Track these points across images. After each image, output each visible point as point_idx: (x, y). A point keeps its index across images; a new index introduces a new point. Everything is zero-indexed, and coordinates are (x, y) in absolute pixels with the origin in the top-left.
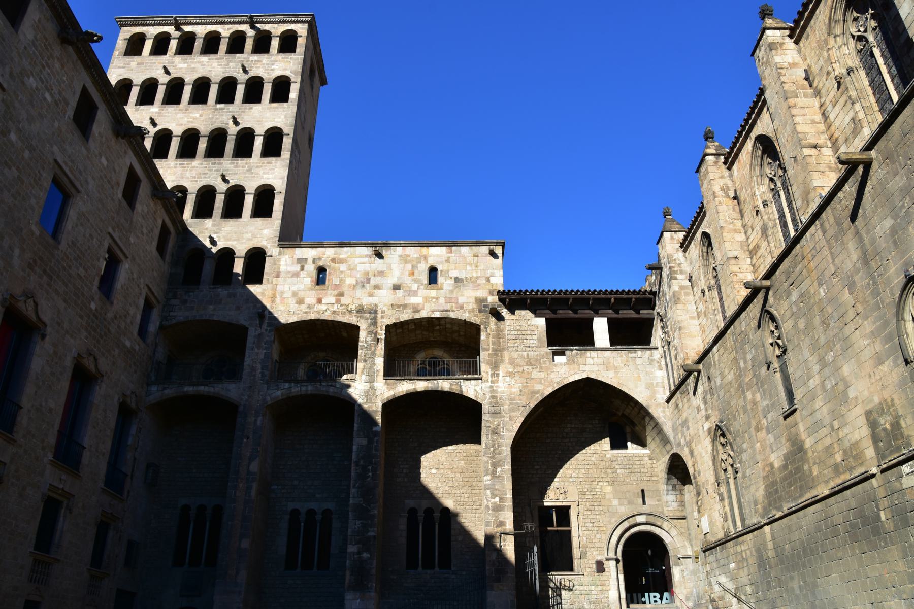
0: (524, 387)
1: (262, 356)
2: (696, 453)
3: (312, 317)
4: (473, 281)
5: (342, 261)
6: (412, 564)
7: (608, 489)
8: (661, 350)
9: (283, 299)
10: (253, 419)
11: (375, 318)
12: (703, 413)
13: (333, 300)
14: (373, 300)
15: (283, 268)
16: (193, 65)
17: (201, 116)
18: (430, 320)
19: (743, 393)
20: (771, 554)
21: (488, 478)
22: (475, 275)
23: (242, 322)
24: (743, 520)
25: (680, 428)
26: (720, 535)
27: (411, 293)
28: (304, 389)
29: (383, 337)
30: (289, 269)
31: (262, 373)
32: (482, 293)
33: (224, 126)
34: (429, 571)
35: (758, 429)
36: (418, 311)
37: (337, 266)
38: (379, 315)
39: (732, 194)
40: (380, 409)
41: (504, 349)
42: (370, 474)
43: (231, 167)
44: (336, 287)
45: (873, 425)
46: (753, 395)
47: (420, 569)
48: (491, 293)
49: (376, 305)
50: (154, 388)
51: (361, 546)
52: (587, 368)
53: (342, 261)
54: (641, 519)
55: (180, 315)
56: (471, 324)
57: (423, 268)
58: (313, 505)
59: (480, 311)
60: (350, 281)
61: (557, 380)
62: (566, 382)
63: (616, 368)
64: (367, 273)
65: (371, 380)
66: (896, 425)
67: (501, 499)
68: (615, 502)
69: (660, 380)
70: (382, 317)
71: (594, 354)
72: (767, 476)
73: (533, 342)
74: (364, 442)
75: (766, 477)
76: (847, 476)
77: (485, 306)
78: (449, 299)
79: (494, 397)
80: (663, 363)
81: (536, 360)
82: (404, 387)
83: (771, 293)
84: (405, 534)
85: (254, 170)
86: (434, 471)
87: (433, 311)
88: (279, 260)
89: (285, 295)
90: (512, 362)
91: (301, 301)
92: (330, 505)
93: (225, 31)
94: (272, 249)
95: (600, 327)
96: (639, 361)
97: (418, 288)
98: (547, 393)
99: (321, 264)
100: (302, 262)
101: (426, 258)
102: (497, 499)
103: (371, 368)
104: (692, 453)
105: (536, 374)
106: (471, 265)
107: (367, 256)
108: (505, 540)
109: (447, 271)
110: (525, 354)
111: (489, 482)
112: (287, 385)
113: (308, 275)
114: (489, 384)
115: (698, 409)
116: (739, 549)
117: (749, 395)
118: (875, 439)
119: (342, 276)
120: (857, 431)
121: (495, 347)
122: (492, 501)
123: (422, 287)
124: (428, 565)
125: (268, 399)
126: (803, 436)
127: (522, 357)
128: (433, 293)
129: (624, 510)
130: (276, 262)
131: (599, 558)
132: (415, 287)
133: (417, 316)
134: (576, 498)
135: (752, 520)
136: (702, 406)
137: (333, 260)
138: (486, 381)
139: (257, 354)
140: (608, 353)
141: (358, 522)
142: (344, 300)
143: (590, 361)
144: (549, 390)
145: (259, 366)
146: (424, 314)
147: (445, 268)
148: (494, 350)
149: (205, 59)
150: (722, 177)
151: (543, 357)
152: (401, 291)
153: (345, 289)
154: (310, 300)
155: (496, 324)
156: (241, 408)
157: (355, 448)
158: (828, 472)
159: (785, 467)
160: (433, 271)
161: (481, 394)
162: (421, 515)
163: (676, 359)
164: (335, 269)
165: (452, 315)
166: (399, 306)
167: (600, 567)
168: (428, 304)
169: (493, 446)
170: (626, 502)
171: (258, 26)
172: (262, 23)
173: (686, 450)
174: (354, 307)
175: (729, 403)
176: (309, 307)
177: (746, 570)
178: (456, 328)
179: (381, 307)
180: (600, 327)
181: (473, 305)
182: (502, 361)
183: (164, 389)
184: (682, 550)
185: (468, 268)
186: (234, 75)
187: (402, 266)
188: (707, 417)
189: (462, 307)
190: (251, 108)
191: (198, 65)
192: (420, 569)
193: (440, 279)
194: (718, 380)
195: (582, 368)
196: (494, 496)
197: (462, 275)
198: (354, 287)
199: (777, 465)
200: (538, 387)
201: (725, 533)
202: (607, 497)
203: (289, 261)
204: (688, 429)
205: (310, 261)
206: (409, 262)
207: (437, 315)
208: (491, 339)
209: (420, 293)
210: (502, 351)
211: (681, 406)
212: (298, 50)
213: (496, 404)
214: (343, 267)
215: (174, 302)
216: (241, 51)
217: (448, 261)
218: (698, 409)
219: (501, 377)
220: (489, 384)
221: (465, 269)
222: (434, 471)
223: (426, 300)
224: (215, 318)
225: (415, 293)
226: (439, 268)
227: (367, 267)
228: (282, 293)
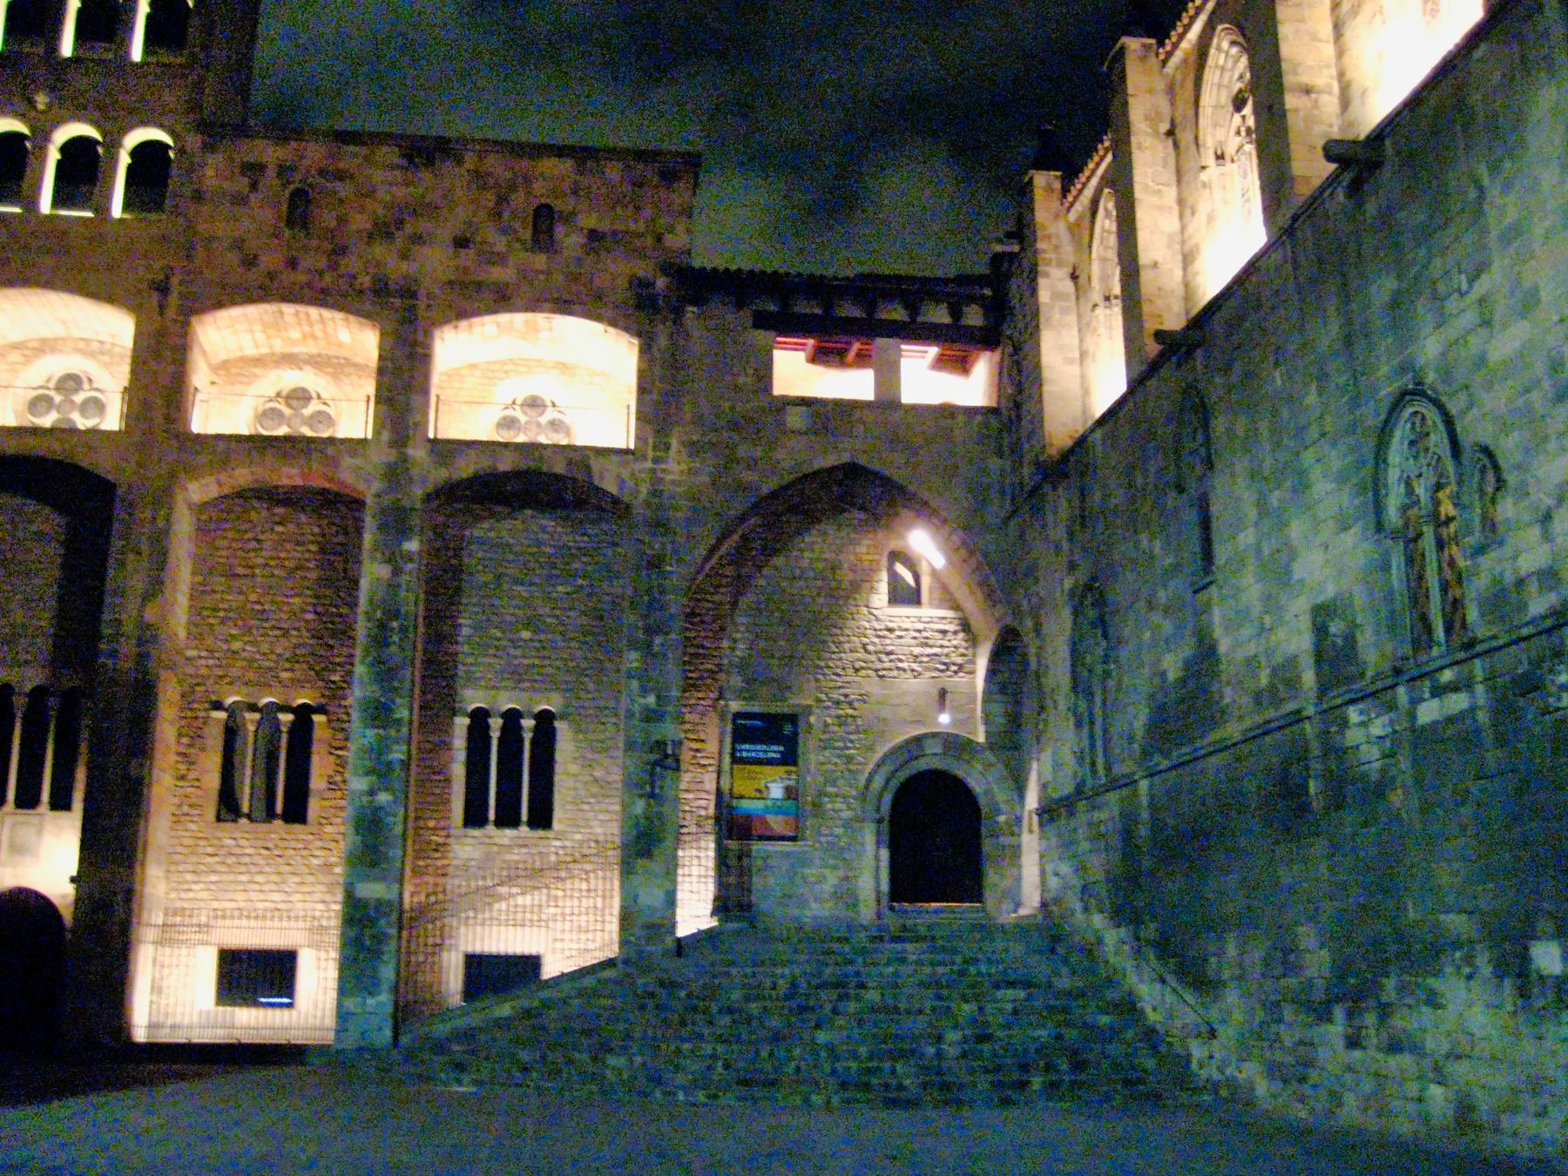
10: (148, 514)
11: (412, 309)
13: (322, 262)
20: (1143, 831)
21: (634, 655)
24: (1108, 768)
32: (643, 269)
35: (1151, 606)
38: (422, 304)
42: (396, 638)
45: (1320, 630)
51: (374, 778)
53: (341, 176)
59: (638, 307)
60: (360, 222)
66: (1350, 639)
67: (658, 697)
74: (385, 571)
75: (1152, 696)
76: (1270, 713)
79: (656, 493)
86: (526, 634)
90: (698, 421)
91: (250, 262)
98: (765, 490)
101: (527, 180)
104: (1037, 630)
108: (663, 777)
110: (727, 405)
111: (635, 665)
114: (649, 465)
118: (1319, 656)
120: (1297, 640)
122: (642, 701)
123: (518, 246)
124: (507, 818)
126: (1218, 632)
128: (540, 261)
132: (500, 243)
136: (1065, 545)
137: (322, 172)
138: (644, 457)
141: (369, 733)
142: (350, 264)
154: (271, 260)
156: (120, 492)
157: (364, 583)
158: (1246, 701)
159: (1183, 681)
166: (464, 285)
173: (1029, 623)
174: (365, 281)
176: (271, 276)
179: (426, 282)
193: (560, 231)
196: (644, 691)
197: (604, 226)
200: (749, 477)
205: (271, 172)
209: (512, 259)
214: (345, 189)
218: (1058, 548)
219: (673, 452)
220: (649, 465)
223: (524, 274)
225: (501, 259)
226: (558, 205)
227: (401, 193)
228: (210, 239)
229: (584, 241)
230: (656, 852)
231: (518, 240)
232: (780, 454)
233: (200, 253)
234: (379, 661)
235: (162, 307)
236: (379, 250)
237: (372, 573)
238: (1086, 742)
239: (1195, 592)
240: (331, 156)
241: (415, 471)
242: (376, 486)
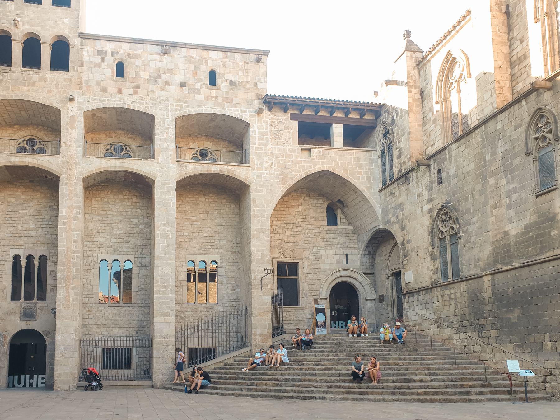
5: (136, 57)
8: (379, 153)
15: (86, 58)
30: (92, 59)
37: (132, 60)
53: (136, 57)
60: (144, 75)
64: (158, 70)
88: (82, 51)
99: (119, 57)
119: (137, 70)
123: (204, 86)
128: (213, 92)
130: (80, 52)
132: (198, 87)
136: (425, 192)
137: (129, 55)
152: (187, 88)
188: (429, 201)
193: (218, 81)
205: (109, 54)
209: (202, 91)
214: (138, 62)
225: (198, 92)
227: (158, 64)
229: (228, 85)
231: (204, 84)
239: (537, 196)
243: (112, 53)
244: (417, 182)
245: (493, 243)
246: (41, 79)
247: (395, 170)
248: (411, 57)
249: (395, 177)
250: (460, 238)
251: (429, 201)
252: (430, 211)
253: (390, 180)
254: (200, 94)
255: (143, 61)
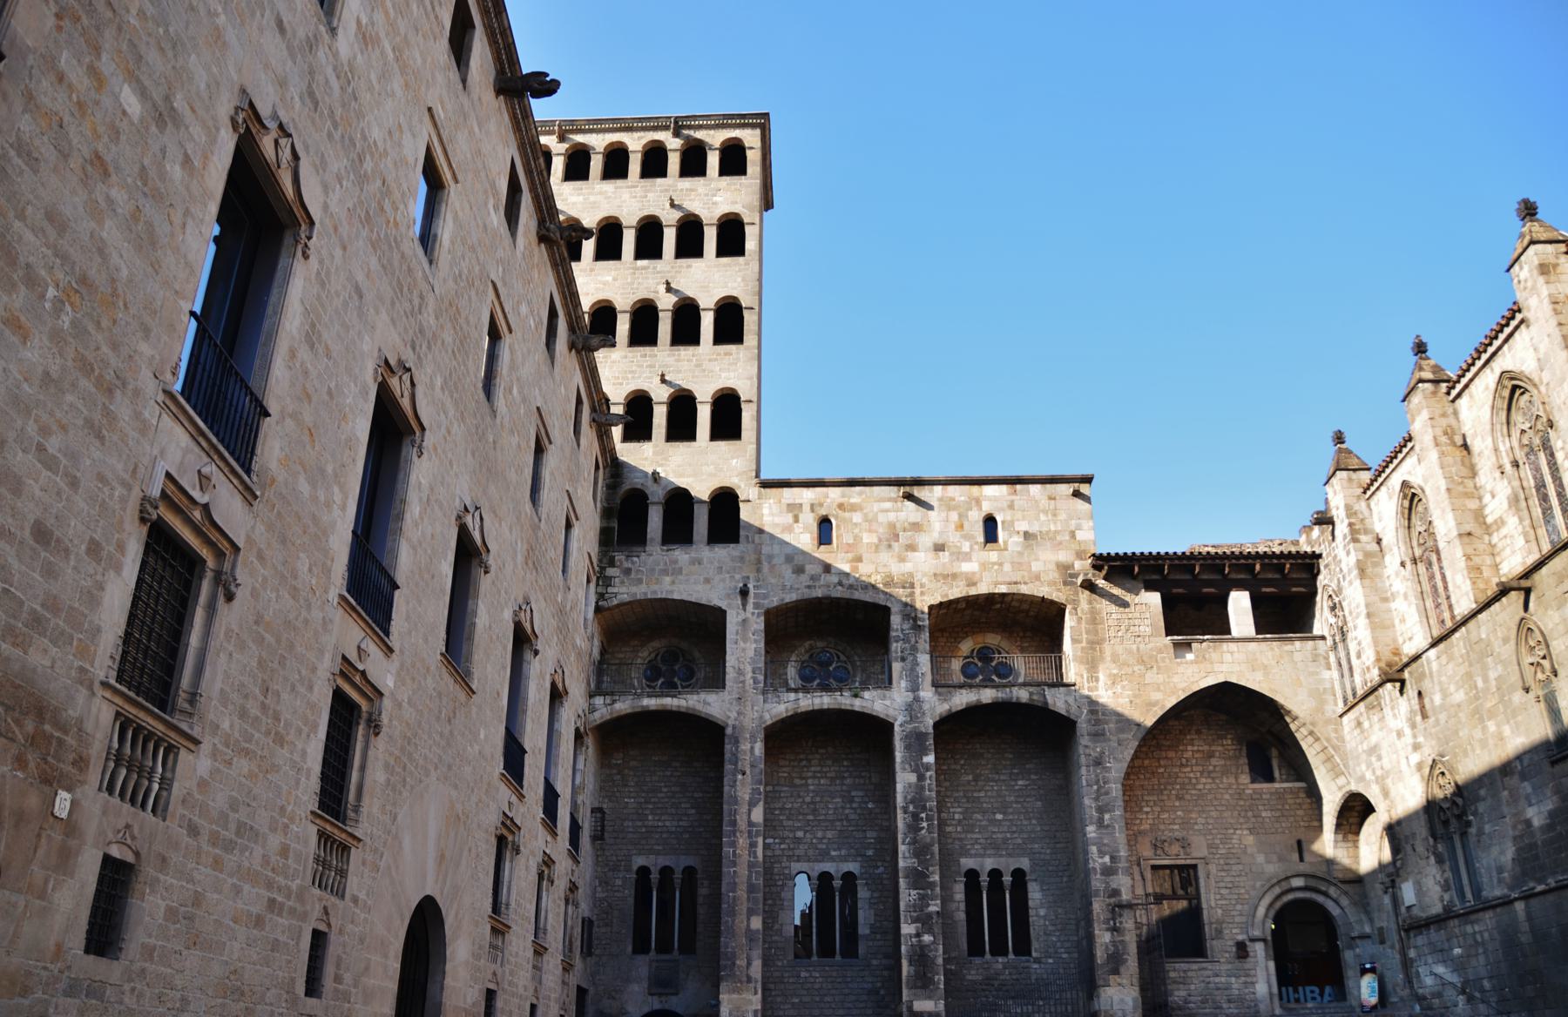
0: (1135, 696)
1: (751, 653)
2: (1393, 793)
3: (819, 593)
4: (1050, 537)
5: (854, 508)
6: (975, 949)
7: (1250, 840)
8: (1329, 642)
9: (772, 567)
12: (1408, 739)
14: (908, 567)
16: (592, 198)
17: (615, 279)
18: (990, 598)
19: (1481, 720)
22: (1053, 528)
23: (716, 602)
24: (1477, 892)
25: (1364, 757)
26: (1437, 909)
27: (962, 556)
28: (817, 701)
29: (927, 623)
30: (777, 520)
31: (756, 681)
32: (1064, 556)
33: (651, 296)
34: (1000, 959)
36: (974, 584)
37: (847, 515)
38: (918, 591)
39: (1459, 442)
40: (931, 730)
41: (1103, 640)
42: (925, 824)
43: (671, 360)
44: (849, 548)
46: (1498, 726)
47: (988, 956)
48: (1080, 555)
49: (911, 575)
50: (599, 701)
52: (1224, 668)
53: (854, 508)
54: (1298, 882)
55: (624, 592)
56: (1052, 602)
57: (976, 518)
58: (829, 867)
59: (1065, 583)
60: (868, 539)
61: (1184, 685)
62: (1196, 688)
63: (1265, 667)
64: (892, 526)
65: (914, 688)
67: (1112, 858)
68: (1260, 859)
69: (1328, 686)
70: (922, 593)
71: (1233, 646)
72: (1521, 837)
73: (1145, 629)
74: (913, 778)
77: (1071, 576)
78: (1017, 566)
79: (1093, 712)
80: (1332, 659)
81: (1151, 657)
82: (962, 699)
83: (1533, 597)
84: (963, 906)
85: (706, 365)
86: (999, 817)
87: (996, 584)
88: (760, 507)
89: (775, 561)
90: (1115, 658)
92: (852, 867)
93: (635, 143)
94: (747, 491)
95: (1239, 605)
96: (1298, 657)
97: (971, 548)
98: (1169, 705)
100: (794, 509)
101: (978, 501)
102: (1107, 859)
103: (913, 670)
105: (1151, 677)
106: (1046, 512)
107: (890, 500)
109: (1012, 523)
112: (792, 696)
113: (806, 529)
115: (1400, 734)
116: (1469, 929)
117: (1492, 726)
121: (1091, 637)
124: (999, 949)
125: (767, 716)
127: (1130, 652)
128: (993, 556)
129: (1273, 869)
131: (1240, 938)
132: (966, 547)
133: (973, 592)
134: (1204, 852)
135: (1494, 891)
136: (1408, 731)
137: (841, 506)
139: (744, 650)
140: (1253, 645)
141: (913, 892)
143: (1228, 657)
144: (1171, 702)
145: (749, 669)
146: (983, 589)
147: (1009, 518)
148: (1089, 642)
149: (610, 186)
150: (1444, 415)
151: (1160, 651)
153: (863, 551)
155: (1090, 602)
156: (729, 731)
157: (899, 787)
159: (1549, 827)
160: (990, 523)
161: (1074, 709)
162: (984, 879)
163: (1359, 656)
164: (844, 520)
165: (1025, 589)
166: (946, 577)
167: (1242, 950)
168: (988, 573)
169: (1097, 782)
170: (1275, 858)
171: (686, 132)
172: (690, 127)
175: (1457, 732)
176: (813, 578)
177: (1482, 959)
178: (1025, 606)
180: (1239, 605)
181: (1054, 575)
182: (1102, 659)
183: (614, 702)
184: (1357, 927)
185: (1043, 518)
186: (657, 212)
187: (944, 515)
188: (1416, 747)
189: (1038, 577)
190: (689, 266)
191: (599, 198)
192: (988, 956)
194: (1437, 699)
195: (1217, 667)
196: (1102, 853)
197: (1034, 528)
198: (877, 548)
199: (1537, 822)
200: (1156, 696)
201: (1444, 908)
202: (1249, 851)
203: (775, 509)
204: (1379, 758)
205: (807, 508)
206: (954, 508)
207: (1003, 589)
208: (1083, 625)
209: (975, 556)
210: (1100, 642)
211: (1366, 725)
212: (749, 170)
213: (1098, 722)
214: (857, 517)
215: (610, 572)
216: (662, 172)
217: (1011, 506)
219: (1101, 683)
221: (1038, 519)
222: (999, 817)
223: (984, 566)
224: (676, 597)
225: (967, 557)
227: (892, 516)
228: (770, 557)
230: (1122, 970)
232: (1176, 679)
233: (766, 567)
234: (914, 842)
235: (744, 605)
236: (884, 556)
237: (904, 779)
238: (1449, 874)
240: (843, 496)
241: (926, 707)
242: (901, 719)
243: (812, 506)
244: (1393, 708)
245: (1515, 838)
246: (694, 562)
247: (1358, 679)
248: (1350, 480)
249: (1360, 692)
250: (1469, 824)
251: (1416, 747)
252: (1420, 767)
253: (1354, 695)
254: (970, 560)
255: (866, 515)
